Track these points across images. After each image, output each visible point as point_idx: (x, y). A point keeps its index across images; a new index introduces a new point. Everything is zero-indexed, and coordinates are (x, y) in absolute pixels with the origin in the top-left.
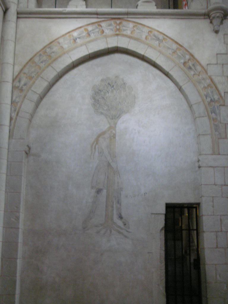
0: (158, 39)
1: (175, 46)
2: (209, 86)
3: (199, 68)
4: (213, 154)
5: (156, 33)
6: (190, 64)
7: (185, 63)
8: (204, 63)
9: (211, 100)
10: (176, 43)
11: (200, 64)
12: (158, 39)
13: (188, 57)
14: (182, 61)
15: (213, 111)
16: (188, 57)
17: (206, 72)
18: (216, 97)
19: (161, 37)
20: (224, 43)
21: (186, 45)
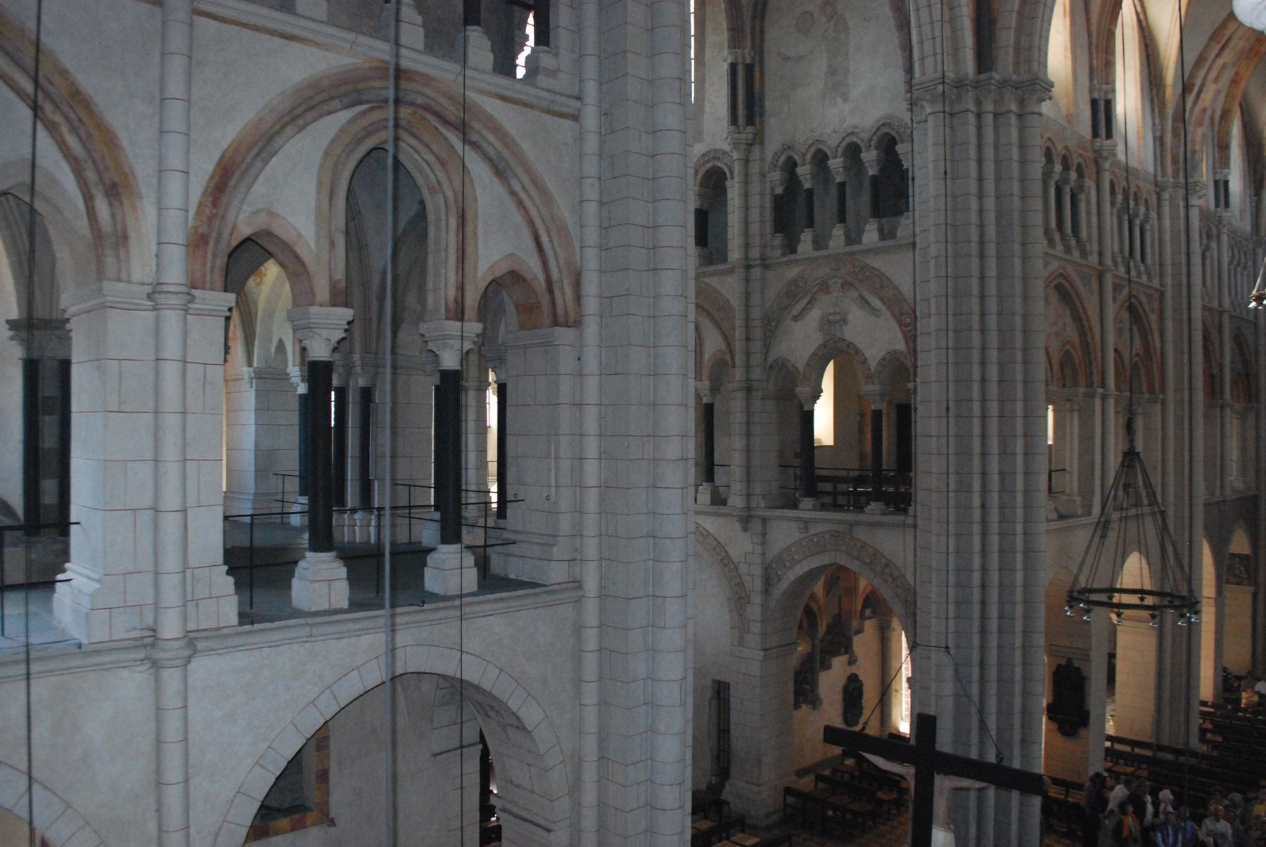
0: (703, 535)
1: (715, 543)
2: (739, 583)
3: (732, 566)
4: (740, 646)
5: (702, 530)
6: (726, 561)
7: (722, 560)
8: (736, 561)
9: (740, 598)
10: (716, 540)
11: (733, 563)
12: (703, 535)
13: (724, 554)
14: (720, 558)
15: (741, 608)
16: (724, 554)
17: (737, 570)
18: (743, 594)
19: (705, 533)
20: (752, 542)
21: (722, 543)
